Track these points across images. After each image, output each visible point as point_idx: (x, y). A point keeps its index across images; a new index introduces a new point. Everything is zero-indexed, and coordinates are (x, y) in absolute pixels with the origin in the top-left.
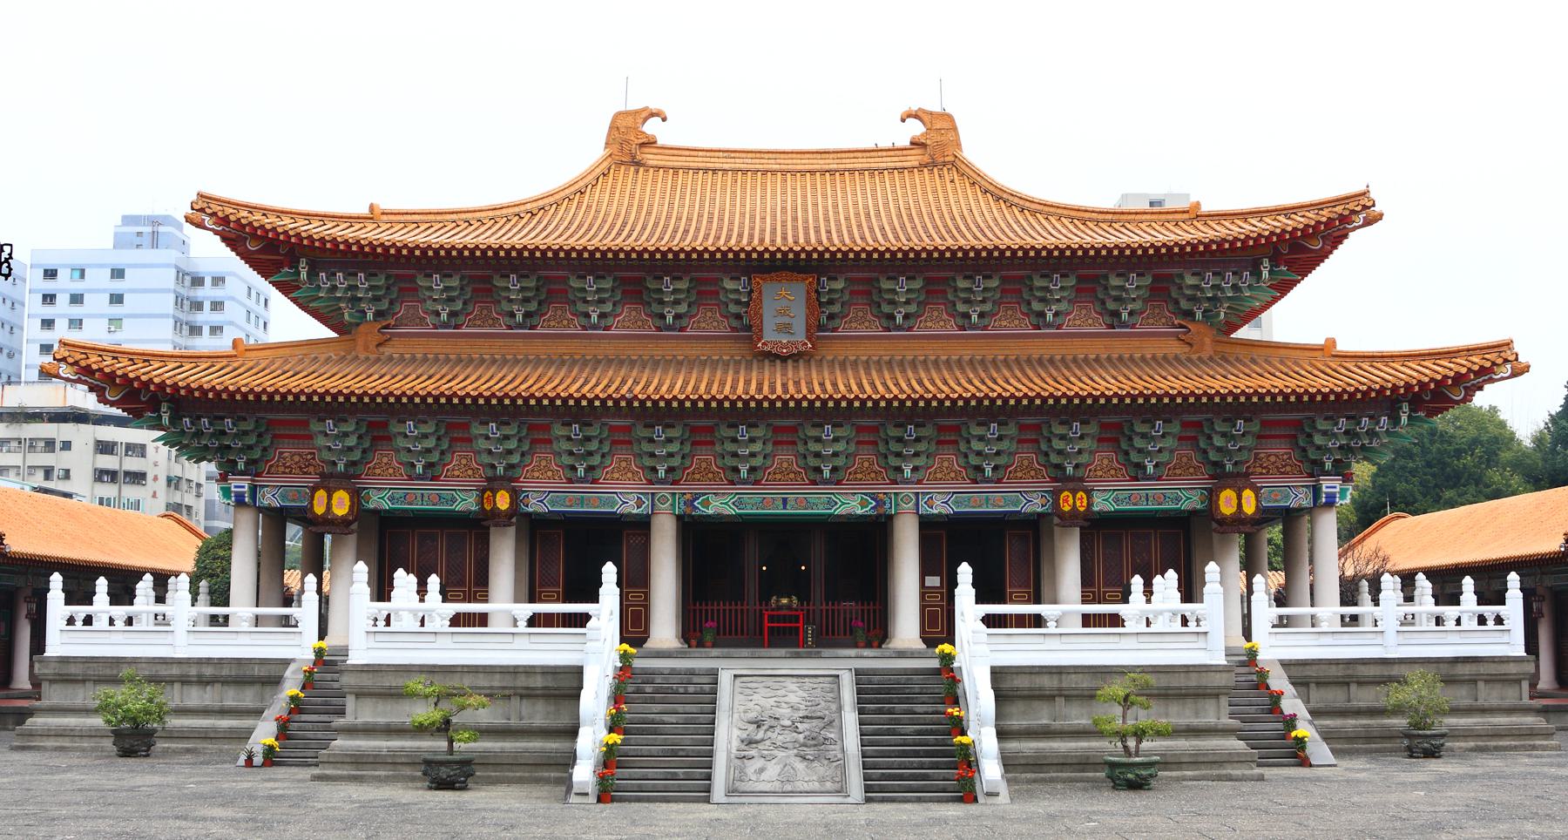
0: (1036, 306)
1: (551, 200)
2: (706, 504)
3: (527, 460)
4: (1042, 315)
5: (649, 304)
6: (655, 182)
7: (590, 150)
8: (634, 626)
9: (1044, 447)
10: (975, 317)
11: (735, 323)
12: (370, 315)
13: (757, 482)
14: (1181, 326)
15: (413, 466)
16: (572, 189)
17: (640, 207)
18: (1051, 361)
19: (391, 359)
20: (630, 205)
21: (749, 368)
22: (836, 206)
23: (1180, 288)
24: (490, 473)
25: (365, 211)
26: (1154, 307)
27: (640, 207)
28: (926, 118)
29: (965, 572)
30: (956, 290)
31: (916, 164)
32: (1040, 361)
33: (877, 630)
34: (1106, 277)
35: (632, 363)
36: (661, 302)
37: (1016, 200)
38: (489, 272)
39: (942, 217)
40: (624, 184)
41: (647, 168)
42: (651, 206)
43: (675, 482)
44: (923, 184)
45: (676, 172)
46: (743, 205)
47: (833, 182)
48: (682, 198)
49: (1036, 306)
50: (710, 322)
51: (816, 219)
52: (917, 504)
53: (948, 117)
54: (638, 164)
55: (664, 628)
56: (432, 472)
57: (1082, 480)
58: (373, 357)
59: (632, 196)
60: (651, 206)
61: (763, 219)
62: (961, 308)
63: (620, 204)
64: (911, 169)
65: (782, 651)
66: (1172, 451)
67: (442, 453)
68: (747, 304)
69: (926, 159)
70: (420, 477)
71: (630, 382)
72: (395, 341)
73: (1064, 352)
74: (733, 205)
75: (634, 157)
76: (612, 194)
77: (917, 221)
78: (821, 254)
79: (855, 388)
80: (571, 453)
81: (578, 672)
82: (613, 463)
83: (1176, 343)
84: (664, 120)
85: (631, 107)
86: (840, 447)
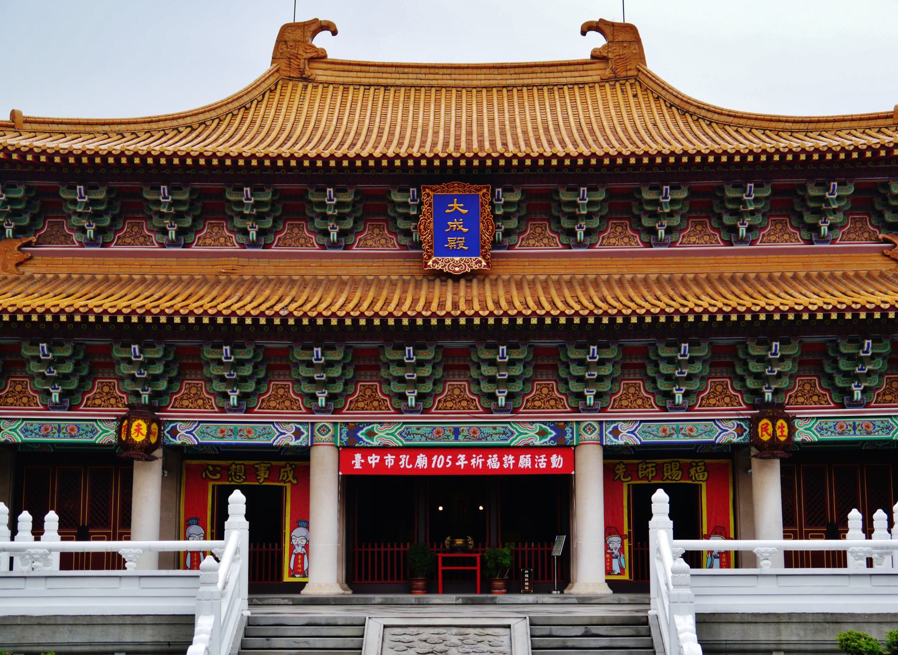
0: (727, 220)
1: (213, 114)
2: (371, 434)
4: (734, 229)
5: (312, 220)
6: (323, 98)
7: (256, 61)
8: (268, 572)
9: (739, 371)
10: (661, 233)
11: (405, 241)
12: (9, 232)
13: (426, 411)
14: (886, 241)
15: (50, 394)
16: (236, 104)
17: (307, 122)
18: (745, 279)
19: (31, 277)
20: (296, 121)
21: (418, 286)
22: (513, 121)
23: (885, 199)
24: (133, 400)
25: (6, 118)
26: (855, 221)
27: (307, 122)
28: (608, 30)
29: (660, 500)
30: (641, 202)
31: (597, 78)
32: (733, 279)
33: (556, 574)
34: (804, 188)
35: (293, 282)
36: (325, 217)
37: (703, 113)
38: (137, 184)
39: (625, 130)
40: (291, 100)
41: (316, 84)
42: (318, 121)
44: (605, 99)
45: (346, 90)
46: (415, 120)
47: (510, 98)
49: (727, 220)
50: (376, 244)
51: (492, 132)
52: (601, 434)
53: (631, 30)
55: (324, 572)
56: (70, 400)
57: (782, 406)
58: (10, 277)
59: (299, 112)
60: (318, 121)
61: (436, 133)
62: (646, 222)
63: (286, 120)
64: (592, 85)
65: (451, 598)
66: (881, 375)
67: (82, 380)
68: (416, 218)
69: (608, 73)
70: (56, 407)
71: (287, 300)
72: (38, 259)
73: (759, 269)
74: (404, 120)
75: (302, 73)
76: (278, 110)
77: (598, 134)
78: (495, 161)
79: (531, 303)
80: (222, 379)
81: (187, 622)
83: (880, 259)
84: (335, 33)
85: (300, 19)
86: (517, 371)
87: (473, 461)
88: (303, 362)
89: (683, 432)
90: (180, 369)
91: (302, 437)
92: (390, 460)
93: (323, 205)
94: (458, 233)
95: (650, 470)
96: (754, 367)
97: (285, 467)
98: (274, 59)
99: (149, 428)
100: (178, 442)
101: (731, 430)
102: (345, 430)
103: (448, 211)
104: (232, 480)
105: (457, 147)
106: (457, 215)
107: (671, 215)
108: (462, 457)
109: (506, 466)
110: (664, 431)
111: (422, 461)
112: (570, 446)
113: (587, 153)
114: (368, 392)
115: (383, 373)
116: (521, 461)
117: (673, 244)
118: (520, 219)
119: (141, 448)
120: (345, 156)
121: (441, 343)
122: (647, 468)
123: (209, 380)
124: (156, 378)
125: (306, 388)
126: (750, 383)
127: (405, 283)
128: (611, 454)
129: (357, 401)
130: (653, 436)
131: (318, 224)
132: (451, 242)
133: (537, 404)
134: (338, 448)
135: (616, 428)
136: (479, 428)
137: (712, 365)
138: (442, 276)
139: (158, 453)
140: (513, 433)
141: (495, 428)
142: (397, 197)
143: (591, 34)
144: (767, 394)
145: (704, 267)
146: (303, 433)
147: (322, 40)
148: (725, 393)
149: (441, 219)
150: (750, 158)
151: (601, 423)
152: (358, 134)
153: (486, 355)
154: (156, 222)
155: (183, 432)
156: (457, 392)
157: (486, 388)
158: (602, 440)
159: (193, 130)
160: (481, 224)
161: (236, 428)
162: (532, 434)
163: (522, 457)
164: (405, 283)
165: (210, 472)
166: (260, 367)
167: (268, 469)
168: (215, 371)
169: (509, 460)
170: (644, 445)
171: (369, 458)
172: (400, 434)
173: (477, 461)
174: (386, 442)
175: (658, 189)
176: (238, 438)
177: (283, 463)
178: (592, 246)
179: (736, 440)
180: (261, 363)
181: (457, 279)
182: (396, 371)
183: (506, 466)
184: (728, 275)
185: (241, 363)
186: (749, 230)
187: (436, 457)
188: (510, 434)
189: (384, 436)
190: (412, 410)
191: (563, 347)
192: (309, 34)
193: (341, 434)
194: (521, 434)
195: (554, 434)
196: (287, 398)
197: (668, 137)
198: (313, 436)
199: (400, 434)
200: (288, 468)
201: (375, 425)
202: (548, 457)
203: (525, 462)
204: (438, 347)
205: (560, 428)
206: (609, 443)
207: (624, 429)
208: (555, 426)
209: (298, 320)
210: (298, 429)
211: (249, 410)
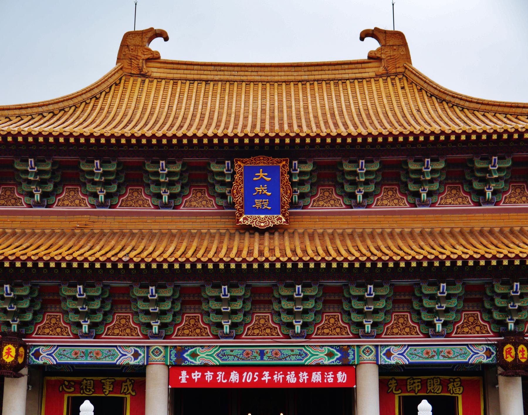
0: (477, 185)
1: (71, 103)
2: (194, 355)
3: (40, 318)
4: (482, 193)
6: (157, 90)
10: (424, 196)
11: (221, 202)
13: (238, 337)
16: (89, 95)
17: (144, 109)
18: (491, 232)
21: (232, 237)
22: (306, 108)
27: (144, 109)
28: (381, 37)
30: (408, 171)
31: (373, 74)
32: (481, 233)
36: (158, 184)
37: (457, 101)
38: (10, 158)
39: (395, 115)
41: (152, 79)
42: (153, 108)
43: (167, 337)
44: (379, 91)
45: (175, 84)
46: (230, 107)
48: (180, 102)
49: (477, 185)
50: (199, 204)
51: (290, 117)
52: (377, 356)
53: (400, 36)
54: (145, 76)
57: (522, 334)
59: (138, 101)
60: (153, 108)
61: (246, 118)
62: (412, 187)
63: (128, 107)
64: (369, 80)
68: (230, 184)
69: (381, 70)
73: (502, 225)
74: (221, 108)
75: (141, 70)
76: (122, 99)
77: (374, 118)
78: (293, 139)
79: (321, 252)
80: (76, 311)
82: (114, 320)
84: (166, 39)
85: (139, 28)
86: (310, 305)
87: (275, 377)
88: (140, 298)
89: (443, 354)
90: (42, 304)
91: (140, 358)
92: (209, 376)
93: (157, 174)
94: (264, 196)
95: (416, 384)
96: (499, 302)
97: (126, 382)
98: (119, 59)
99: (17, 351)
100: (40, 362)
101: (481, 353)
102: (174, 352)
103: (255, 179)
104: (84, 393)
105: (263, 129)
106: (262, 181)
107: (431, 181)
108: (266, 373)
109: (301, 381)
110: (428, 353)
111: (234, 377)
112: (352, 365)
113: (364, 132)
114: (192, 322)
115: (204, 307)
116: (313, 377)
117: (433, 205)
118: (312, 185)
119: (10, 367)
120: (174, 136)
121: (249, 282)
122: (414, 383)
123: (66, 313)
124: (23, 311)
125: (143, 319)
126: (496, 316)
127: (222, 235)
128: (386, 373)
129: (183, 329)
130: (418, 357)
131: (153, 189)
132: (258, 203)
133: (326, 331)
134: (168, 366)
135: (389, 351)
136: (280, 350)
137: (466, 301)
138: (251, 230)
139: (25, 371)
140: (307, 355)
141: (292, 351)
142: (215, 168)
143: (368, 40)
144: (510, 324)
145: (459, 223)
146: (140, 355)
147: (156, 45)
148: (475, 323)
149: (250, 185)
150: (495, 137)
151: (376, 346)
152: (184, 118)
153: (285, 292)
154: (25, 187)
155: (44, 354)
156: (262, 321)
157: (285, 318)
158: (377, 360)
159: (55, 115)
160: (281, 189)
161: (87, 350)
162: (322, 355)
163: (314, 374)
164: (222, 235)
165: (66, 386)
166: (107, 302)
167: (112, 383)
168: (70, 305)
169: (304, 376)
170: (411, 365)
171: (193, 374)
172: (218, 355)
173: (278, 377)
174: (206, 362)
175: (420, 161)
176: (89, 358)
177: (124, 379)
178: (369, 206)
179: (485, 361)
180: (107, 299)
181: (262, 232)
182: (214, 305)
183: (301, 381)
184: (477, 229)
185: (91, 299)
186: (494, 193)
187: (246, 373)
188: (304, 355)
189: (205, 356)
190: (227, 336)
191: (346, 286)
192: (146, 40)
193: (170, 355)
195: (339, 355)
196: (128, 327)
197: (429, 120)
198: (148, 357)
199: (218, 355)
200: (129, 383)
201: (198, 348)
202: (335, 374)
203: (316, 377)
204: (248, 286)
205: (344, 350)
206: (383, 363)
207: (395, 352)
208: (340, 349)
209: (137, 265)
210: (136, 352)
211: (98, 336)
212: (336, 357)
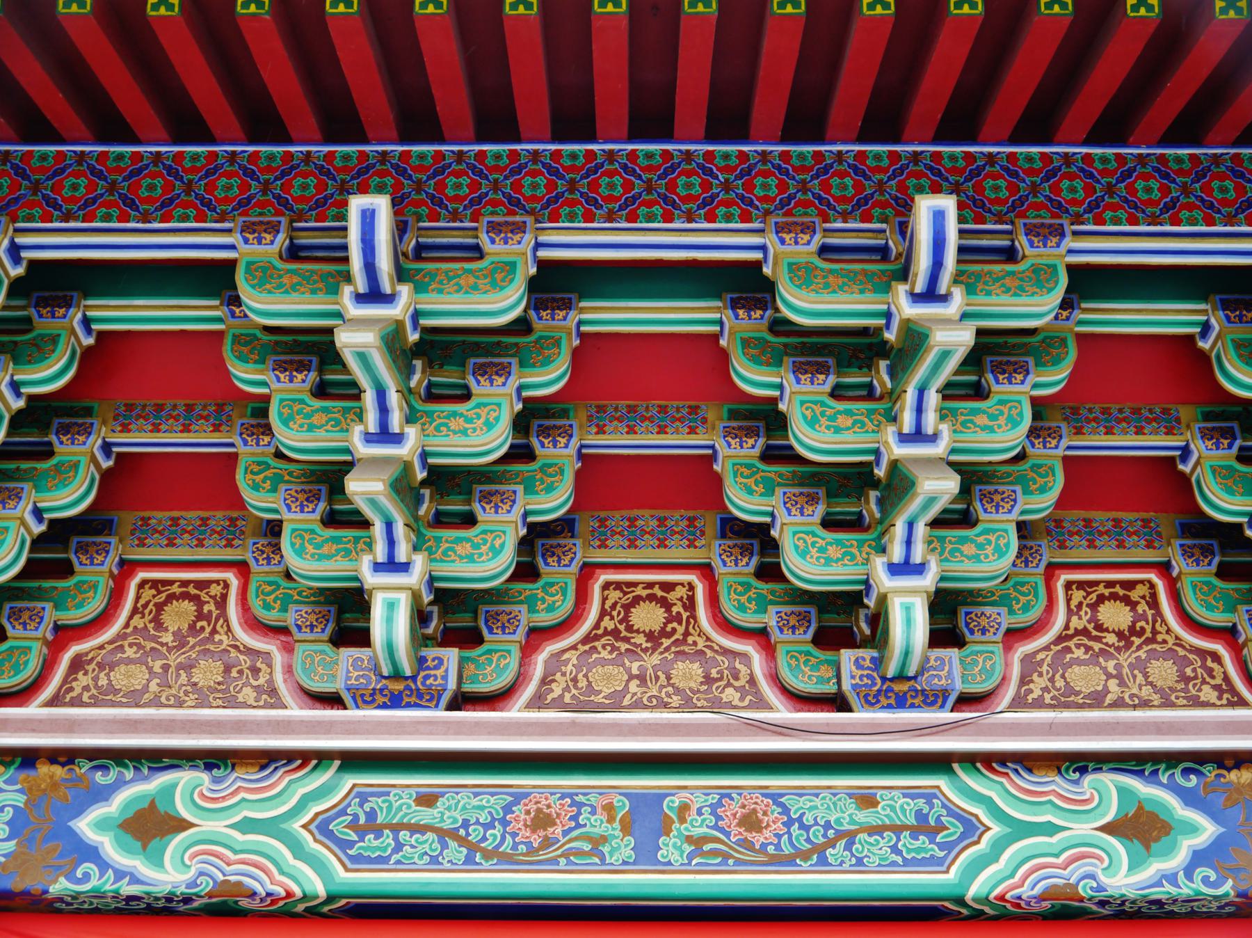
136: (775, 798)
140: (972, 830)
162: (1083, 829)
172: (322, 827)
188: (955, 829)
194: (1023, 830)
195: (1208, 830)
212: (1185, 848)
